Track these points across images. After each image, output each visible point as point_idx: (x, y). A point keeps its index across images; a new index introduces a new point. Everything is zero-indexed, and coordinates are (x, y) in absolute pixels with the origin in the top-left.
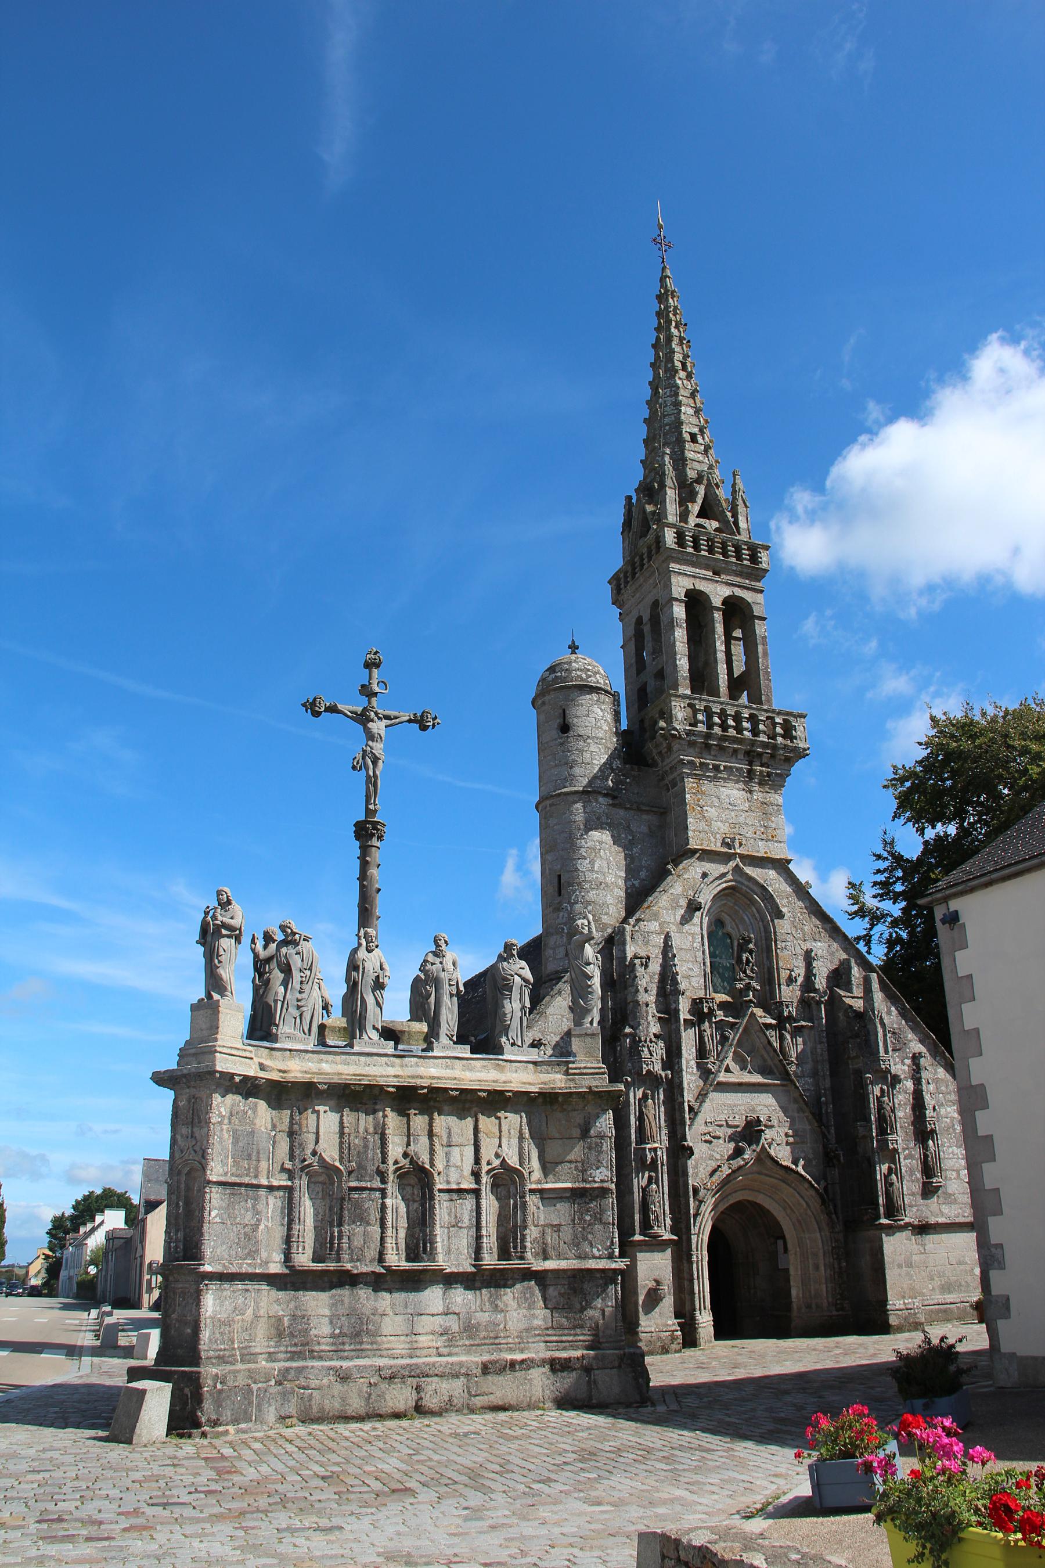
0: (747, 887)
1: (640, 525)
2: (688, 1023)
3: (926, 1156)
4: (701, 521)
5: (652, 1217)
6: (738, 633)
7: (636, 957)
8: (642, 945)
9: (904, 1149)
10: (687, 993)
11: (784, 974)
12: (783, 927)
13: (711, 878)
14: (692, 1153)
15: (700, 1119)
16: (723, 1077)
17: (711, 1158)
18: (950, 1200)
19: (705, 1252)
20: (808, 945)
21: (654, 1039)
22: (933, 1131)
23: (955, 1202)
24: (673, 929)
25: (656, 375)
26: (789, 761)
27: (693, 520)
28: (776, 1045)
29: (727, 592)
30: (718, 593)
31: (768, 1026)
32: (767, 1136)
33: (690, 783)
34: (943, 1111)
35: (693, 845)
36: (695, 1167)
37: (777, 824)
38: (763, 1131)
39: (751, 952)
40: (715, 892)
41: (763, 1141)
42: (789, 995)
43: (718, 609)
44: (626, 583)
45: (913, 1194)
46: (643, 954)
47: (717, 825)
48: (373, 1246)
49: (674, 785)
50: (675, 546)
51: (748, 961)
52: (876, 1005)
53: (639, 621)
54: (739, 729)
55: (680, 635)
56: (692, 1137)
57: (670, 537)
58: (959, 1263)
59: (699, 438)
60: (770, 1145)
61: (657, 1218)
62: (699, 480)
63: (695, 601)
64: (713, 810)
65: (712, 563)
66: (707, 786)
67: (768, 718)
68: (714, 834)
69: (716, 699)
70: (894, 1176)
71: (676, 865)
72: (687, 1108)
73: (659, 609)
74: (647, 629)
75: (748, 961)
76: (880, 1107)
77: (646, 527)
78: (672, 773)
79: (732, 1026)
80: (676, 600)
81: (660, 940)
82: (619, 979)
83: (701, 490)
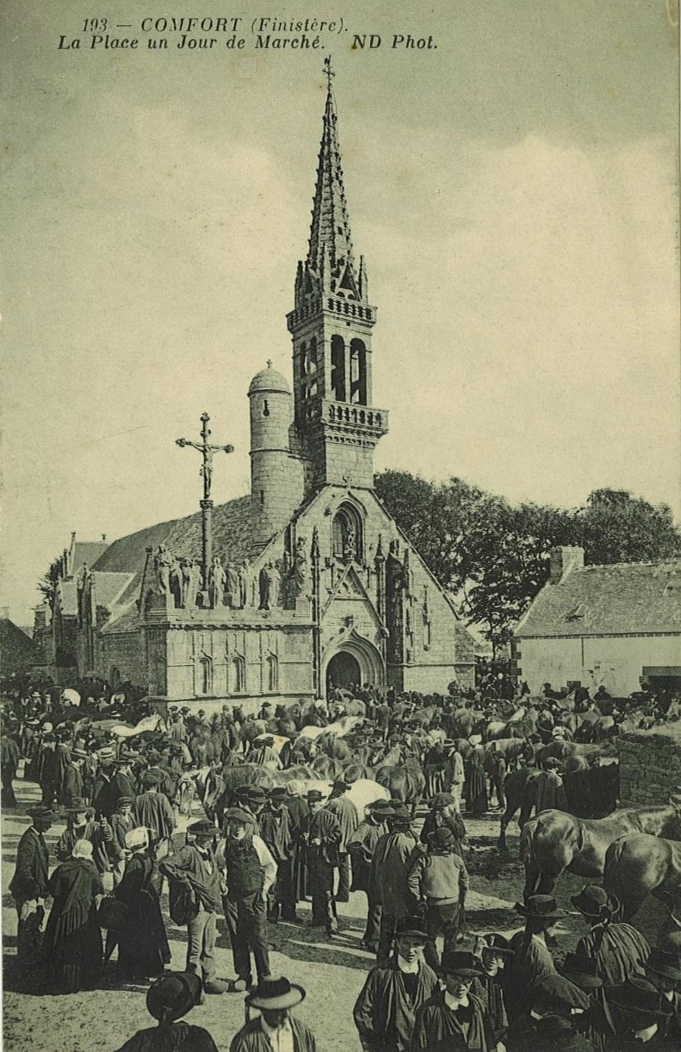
1: (306, 283)
4: (341, 290)
6: (355, 356)
8: (304, 530)
12: (368, 522)
25: (320, 180)
26: (378, 436)
30: (348, 336)
35: (327, 482)
39: (353, 535)
50: (328, 309)
51: (351, 540)
63: (337, 341)
65: (348, 318)
71: (320, 491)
73: (316, 344)
75: (351, 540)
77: (309, 289)
79: (342, 571)
81: (311, 530)
82: (292, 546)
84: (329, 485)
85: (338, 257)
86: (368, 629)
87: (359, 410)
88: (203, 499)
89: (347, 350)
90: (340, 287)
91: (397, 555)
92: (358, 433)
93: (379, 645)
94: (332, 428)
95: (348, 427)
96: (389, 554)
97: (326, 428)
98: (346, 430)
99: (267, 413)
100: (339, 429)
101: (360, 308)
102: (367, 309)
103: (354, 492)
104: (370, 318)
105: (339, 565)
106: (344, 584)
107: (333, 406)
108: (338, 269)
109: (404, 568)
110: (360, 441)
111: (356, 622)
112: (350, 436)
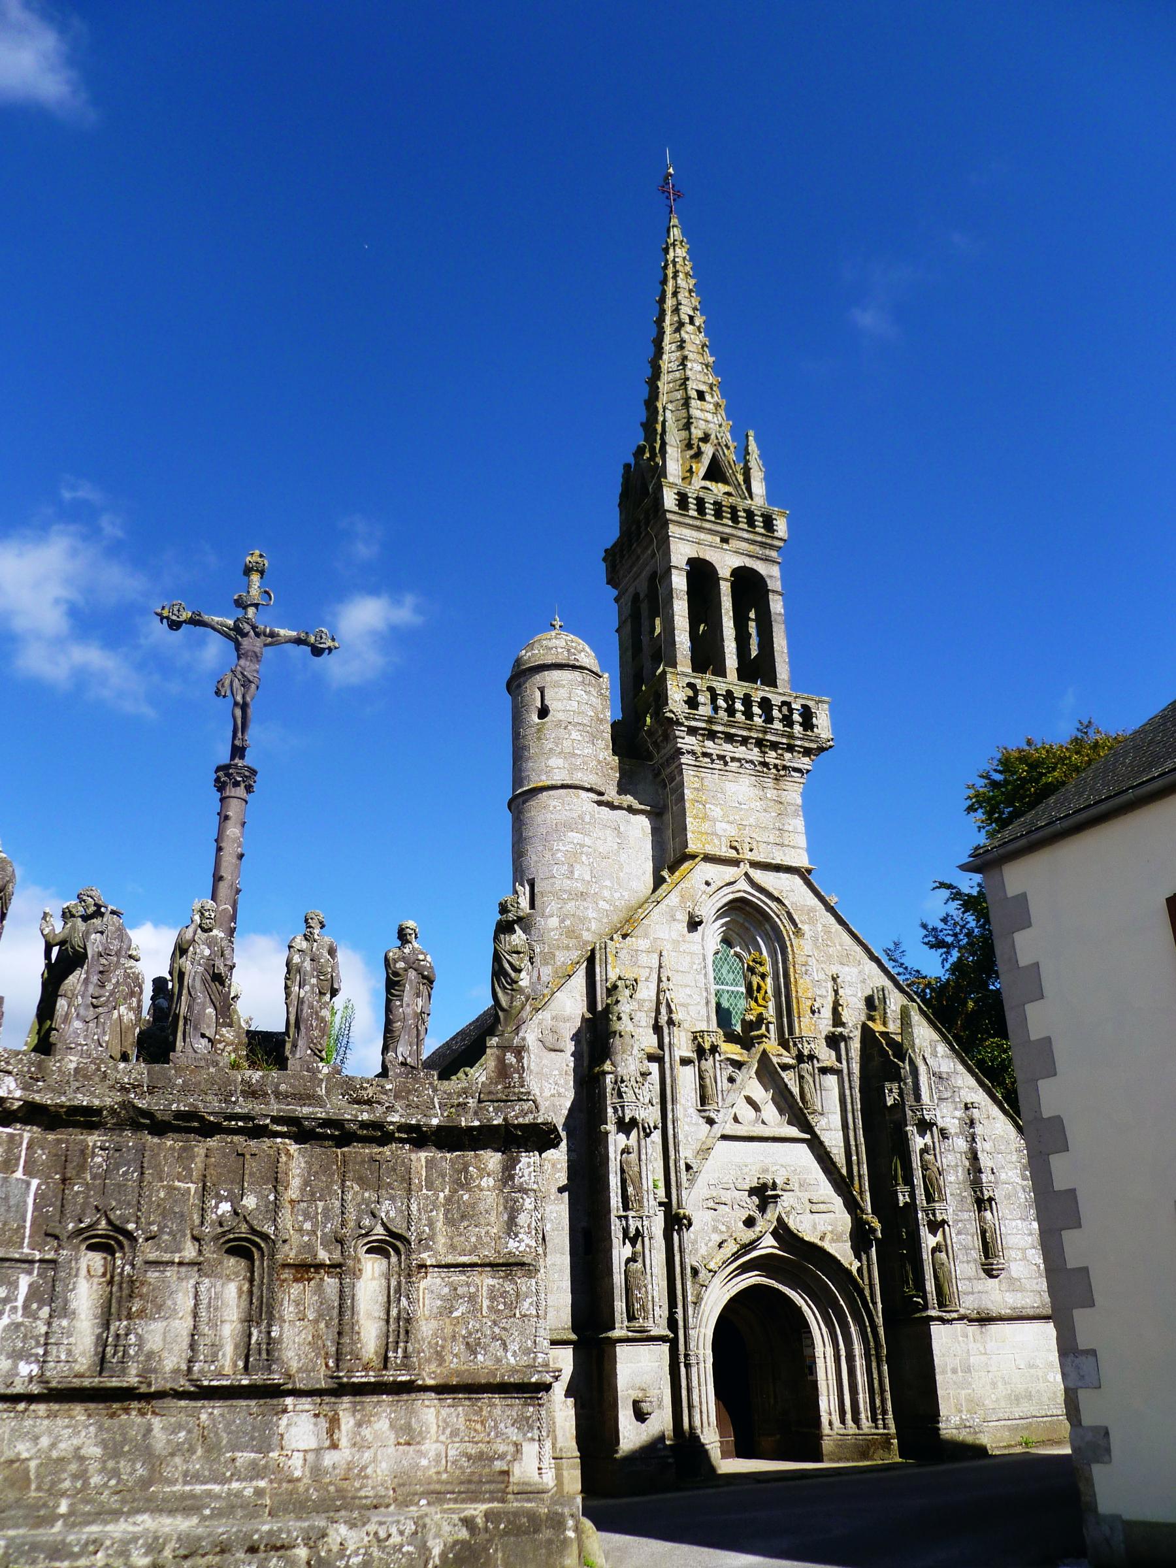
0: (759, 899)
2: (685, 1062)
3: (984, 1232)
4: (708, 484)
5: (637, 1306)
7: (620, 978)
9: (956, 1222)
10: (685, 1025)
11: (805, 1005)
12: (802, 949)
13: (714, 887)
14: (690, 1224)
15: (701, 1180)
16: (731, 1129)
17: (715, 1230)
18: (1014, 1285)
19: (709, 1352)
20: (834, 969)
21: (640, 1079)
22: (991, 1199)
23: (1022, 1290)
24: (667, 948)
27: (698, 482)
28: (796, 1090)
29: (738, 562)
30: (726, 562)
31: (785, 1067)
32: (785, 1204)
33: (689, 776)
34: (1003, 1176)
35: (692, 847)
36: (695, 1242)
37: (795, 828)
38: (778, 1196)
40: (720, 905)
41: (779, 1209)
42: (813, 1028)
43: (726, 580)
44: (622, 557)
45: (969, 1279)
46: (630, 975)
47: (721, 827)
48: (176, 1348)
49: (673, 779)
50: (676, 509)
52: (917, 1041)
53: (636, 598)
54: (749, 715)
55: (681, 608)
56: (692, 1202)
57: (670, 500)
58: (1031, 1366)
59: (708, 397)
60: (788, 1214)
61: (643, 1308)
62: (706, 438)
63: (701, 572)
64: (718, 809)
66: (711, 779)
67: (784, 703)
68: (719, 837)
69: (720, 679)
70: (943, 1255)
72: (683, 1167)
74: (644, 607)
76: (925, 1168)
78: (668, 765)
79: (738, 1065)
80: (676, 567)
83: (708, 450)
84: (693, 857)
85: (697, 433)
86: (824, 1221)
87: (757, 696)
88: (225, 759)
89: (725, 588)
90: (704, 478)
91: (885, 1024)
92: (760, 743)
93: (856, 1264)
94: (692, 731)
95: (733, 731)
96: (864, 1027)
97: (680, 732)
98: (730, 738)
99: (543, 712)
100: (712, 735)
101: (750, 515)
102: (762, 515)
103: (758, 876)
104: (773, 531)
105: (733, 1051)
106: (750, 1101)
107: (691, 685)
108: (699, 448)
109: (900, 1051)
110: (765, 764)
111: (787, 1200)
112: (741, 751)
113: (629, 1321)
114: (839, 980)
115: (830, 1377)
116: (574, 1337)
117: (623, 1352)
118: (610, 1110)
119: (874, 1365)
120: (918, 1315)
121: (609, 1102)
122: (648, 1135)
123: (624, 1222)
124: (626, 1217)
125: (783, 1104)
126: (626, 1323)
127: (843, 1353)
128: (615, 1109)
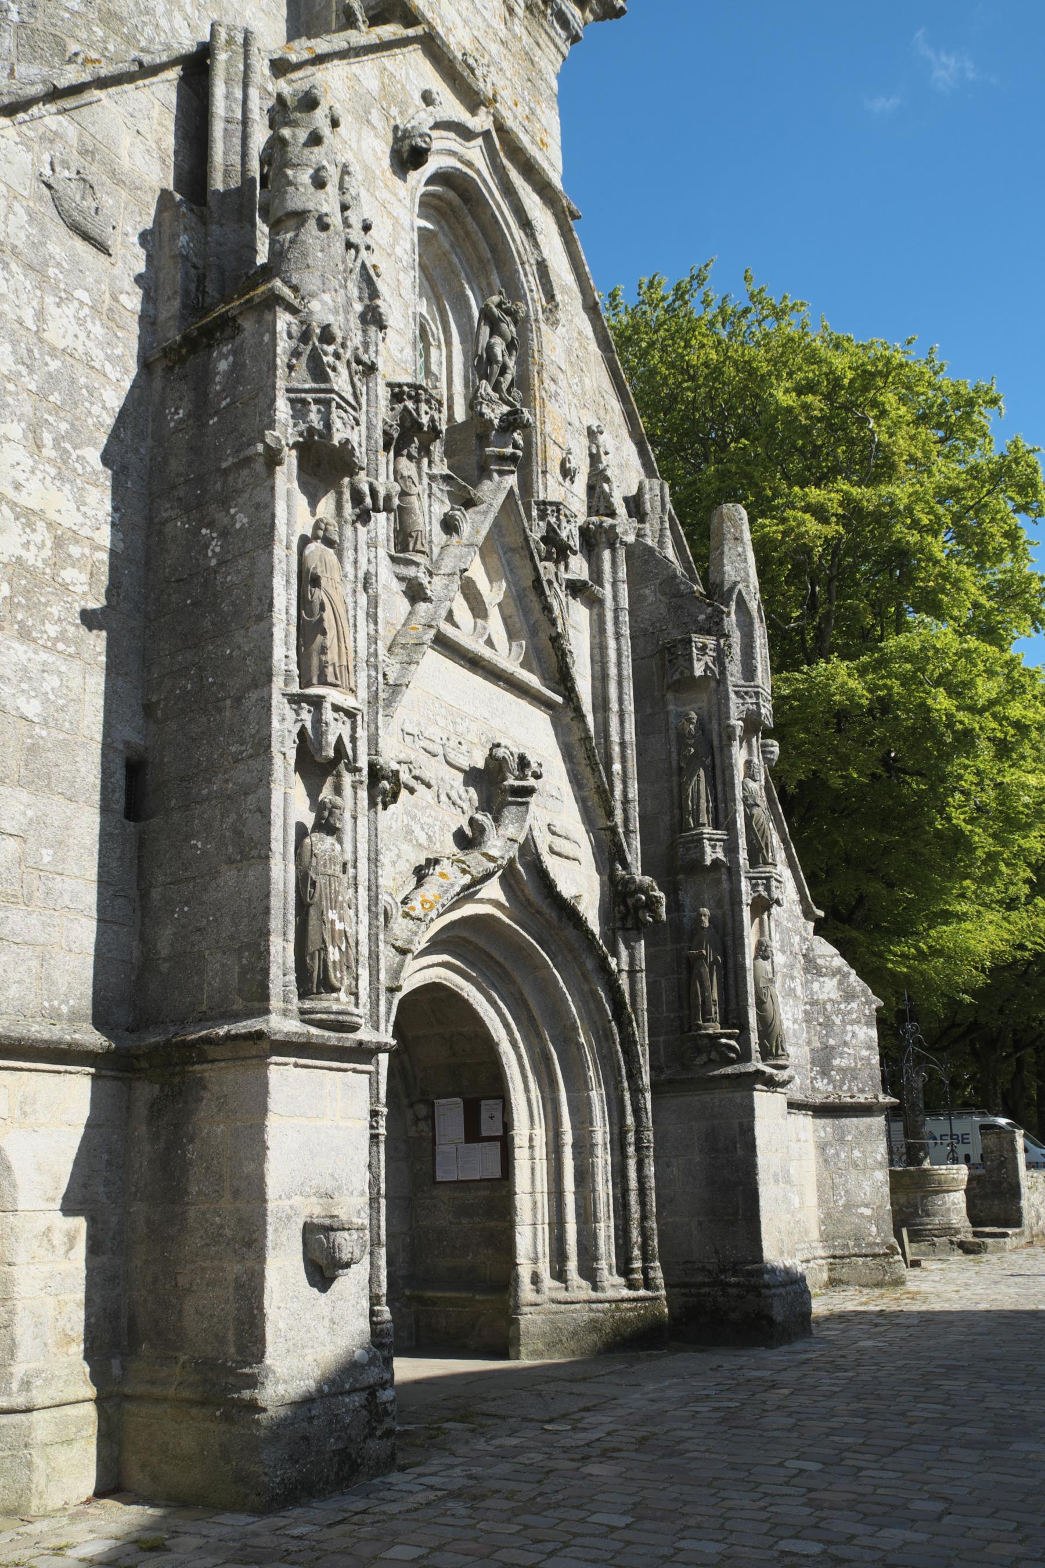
113: (301, 997)
114: (601, 439)
115: (539, 1188)
116: (94, 1039)
117: (285, 1079)
118: (283, 409)
119: (632, 1164)
120: (729, 1070)
121: (281, 384)
122: (364, 517)
123: (307, 717)
124: (317, 703)
125: (518, 621)
126: (295, 1003)
127: (568, 1138)
128: (299, 407)
